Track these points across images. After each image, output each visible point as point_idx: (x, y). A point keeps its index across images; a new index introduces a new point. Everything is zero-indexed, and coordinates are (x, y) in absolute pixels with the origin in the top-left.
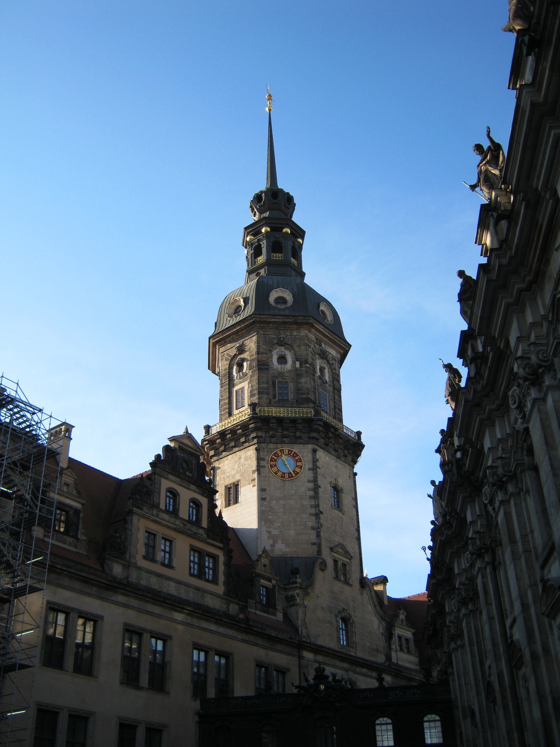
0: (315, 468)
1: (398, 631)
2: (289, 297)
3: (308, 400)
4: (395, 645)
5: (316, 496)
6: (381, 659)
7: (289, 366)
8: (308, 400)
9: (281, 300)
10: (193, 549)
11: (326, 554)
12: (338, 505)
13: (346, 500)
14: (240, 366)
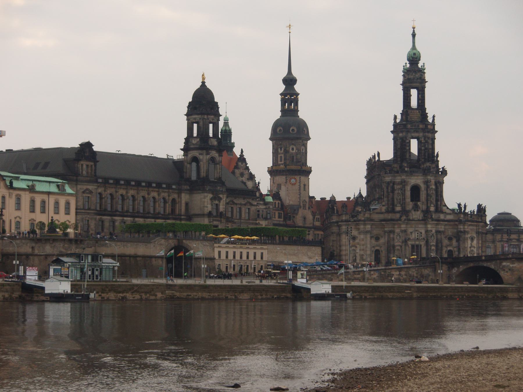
0: (300, 182)
1: (316, 217)
2: (296, 129)
3: (299, 162)
4: (315, 220)
5: (300, 190)
6: (311, 225)
7: (294, 151)
8: (299, 162)
9: (293, 130)
10: (279, 213)
11: (302, 205)
12: (305, 190)
13: (307, 187)
14: (281, 149)
